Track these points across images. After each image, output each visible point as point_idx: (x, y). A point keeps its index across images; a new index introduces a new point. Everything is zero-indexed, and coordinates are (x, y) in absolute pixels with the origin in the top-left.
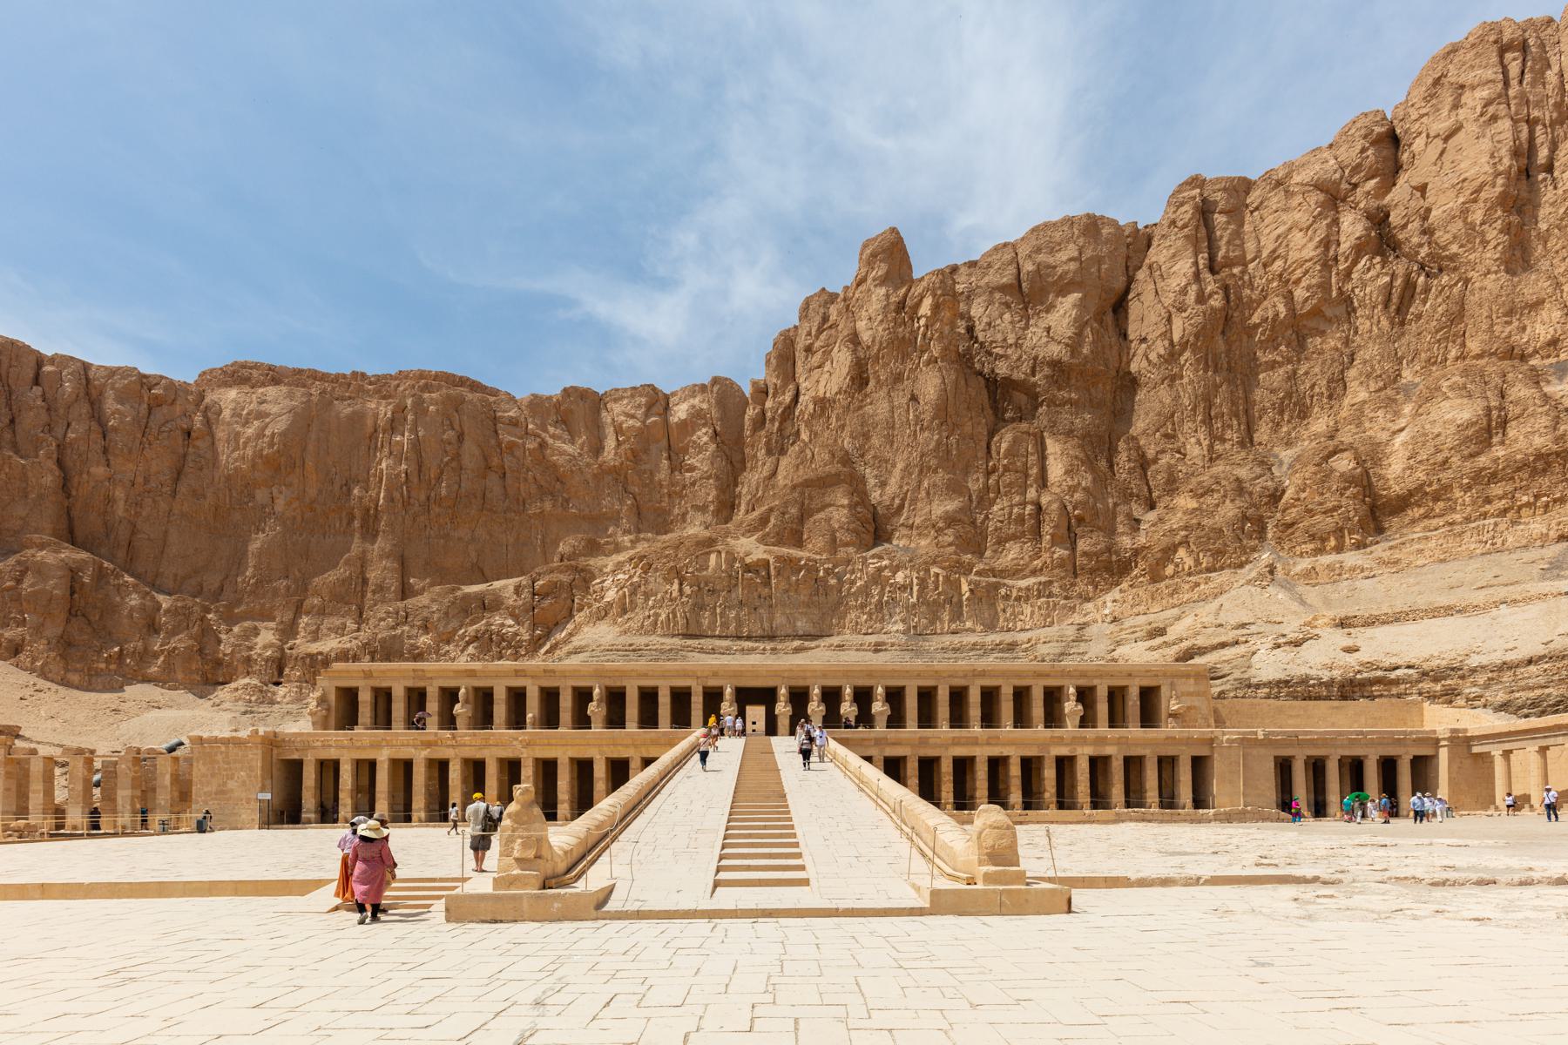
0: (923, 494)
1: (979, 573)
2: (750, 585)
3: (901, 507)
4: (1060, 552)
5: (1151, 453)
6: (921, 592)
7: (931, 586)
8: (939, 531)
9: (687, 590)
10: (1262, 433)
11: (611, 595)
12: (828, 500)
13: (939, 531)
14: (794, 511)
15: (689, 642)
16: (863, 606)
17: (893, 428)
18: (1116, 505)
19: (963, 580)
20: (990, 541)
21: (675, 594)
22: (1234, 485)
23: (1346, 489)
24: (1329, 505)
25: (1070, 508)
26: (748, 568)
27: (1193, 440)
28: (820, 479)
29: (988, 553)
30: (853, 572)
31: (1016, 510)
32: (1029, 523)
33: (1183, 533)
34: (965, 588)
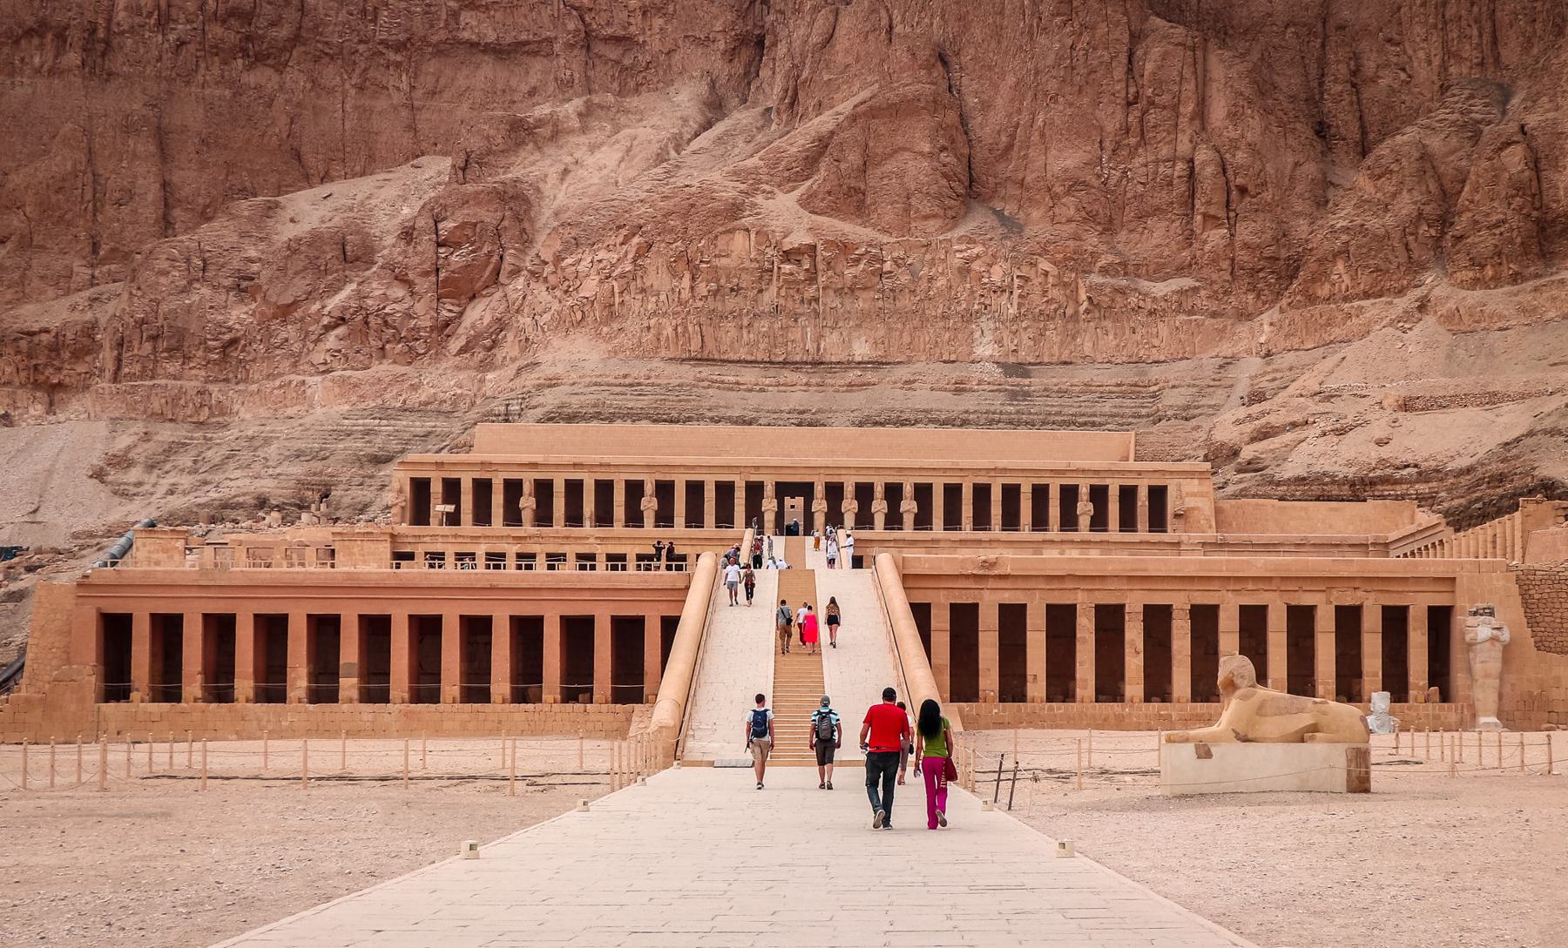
0: (1035, 138)
1: (1104, 271)
2: (791, 283)
3: (1009, 147)
4: (1215, 237)
5: (1369, 65)
6: (1020, 296)
7: (1038, 290)
8: (1055, 197)
9: (702, 289)
10: (1511, 53)
11: (590, 287)
12: (900, 141)
13: (1055, 197)
14: (854, 158)
15: (706, 371)
16: (945, 317)
17: (1001, 13)
18: (1297, 164)
19: (1081, 284)
20: (1130, 213)
21: (686, 295)
22: (1416, 165)
23: (1513, 197)
24: (1494, 218)
25: (1230, 172)
26: (788, 256)
27: (1421, 54)
28: (890, 106)
29: (1123, 236)
30: (932, 263)
31: (1161, 170)
32: (1181, 188)
33: (1345, 238)
34: (1083, 296)
